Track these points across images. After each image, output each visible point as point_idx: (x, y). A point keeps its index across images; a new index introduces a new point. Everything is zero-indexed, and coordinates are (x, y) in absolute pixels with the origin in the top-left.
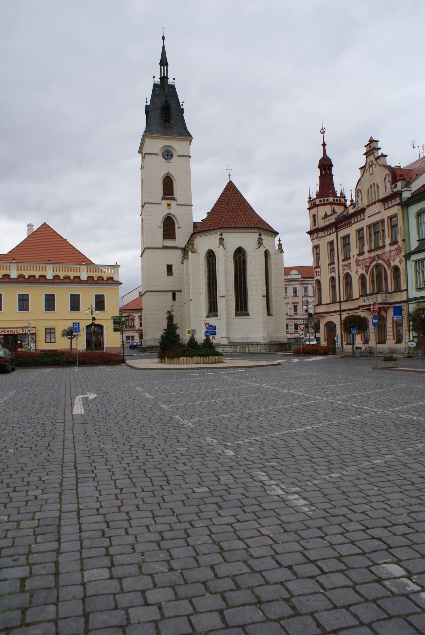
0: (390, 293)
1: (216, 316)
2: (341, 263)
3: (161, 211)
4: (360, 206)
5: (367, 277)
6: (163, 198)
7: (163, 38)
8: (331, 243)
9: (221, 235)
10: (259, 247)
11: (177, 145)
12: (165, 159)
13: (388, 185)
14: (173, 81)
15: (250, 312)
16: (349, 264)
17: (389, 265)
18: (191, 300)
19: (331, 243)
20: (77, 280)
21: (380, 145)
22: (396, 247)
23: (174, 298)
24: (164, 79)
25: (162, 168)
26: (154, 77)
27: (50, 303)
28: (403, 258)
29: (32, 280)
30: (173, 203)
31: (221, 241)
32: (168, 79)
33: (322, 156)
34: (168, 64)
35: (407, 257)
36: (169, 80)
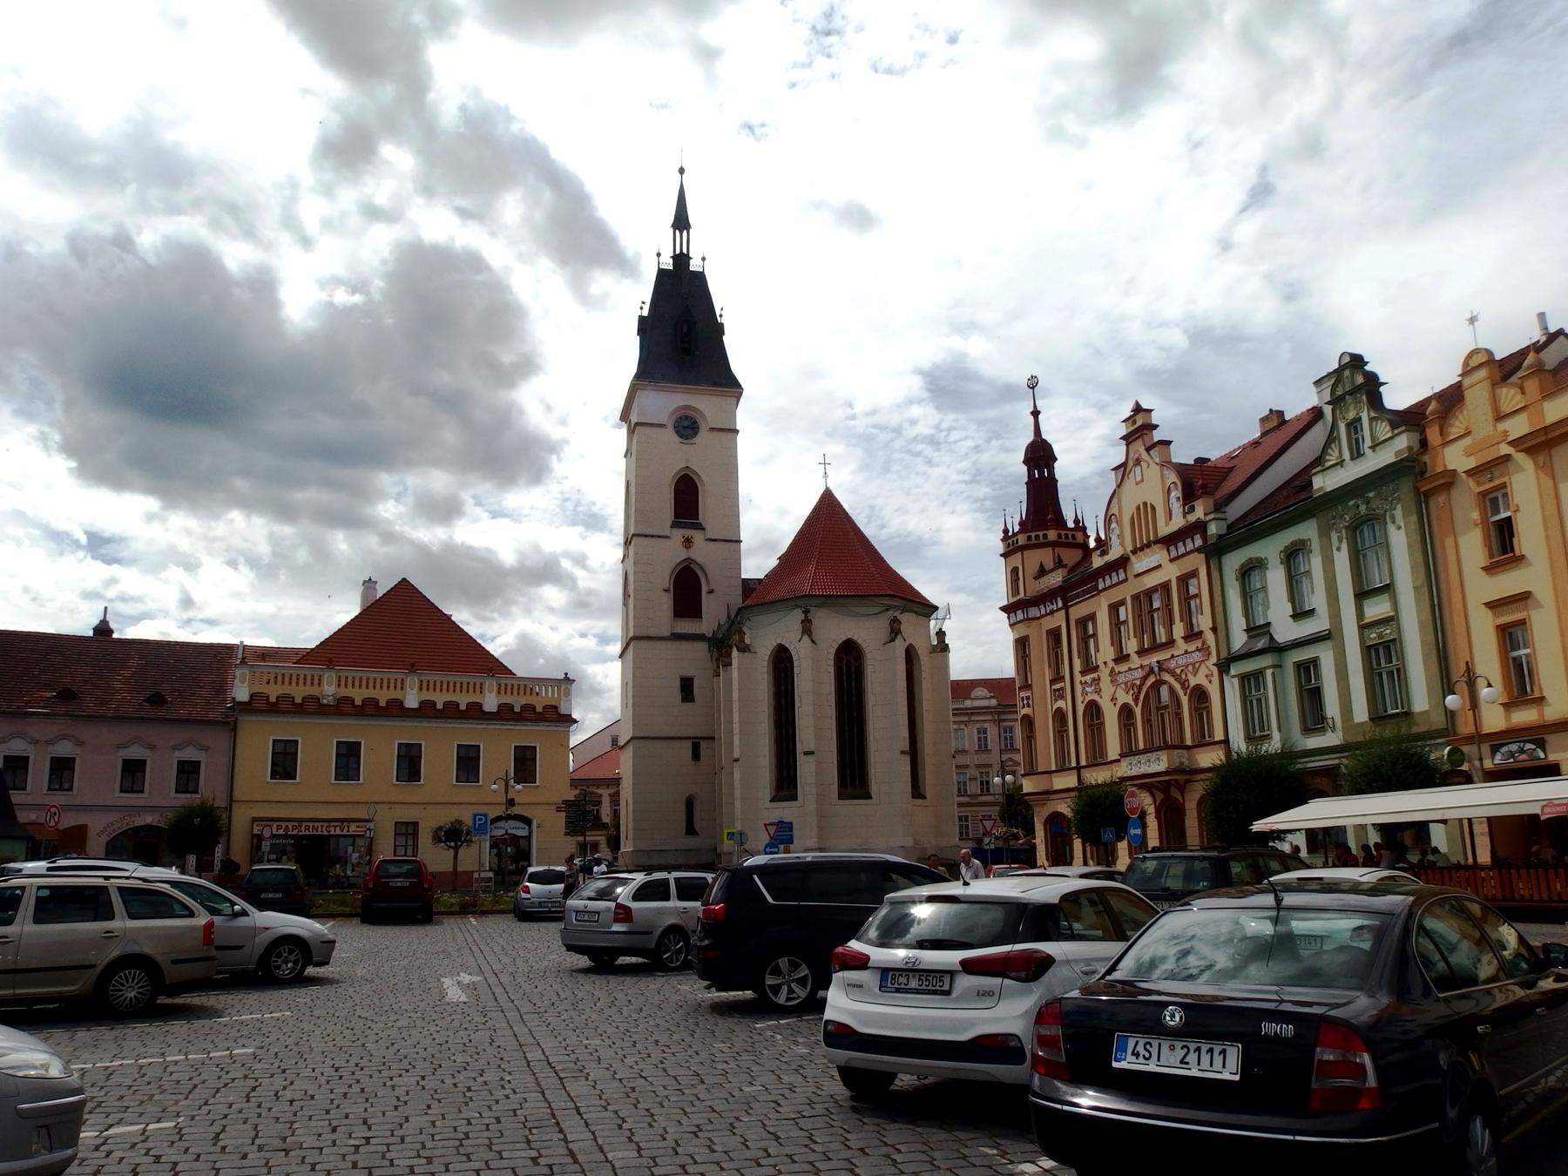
0: (1188, 748)
1: (794, 798)
2: (1078, 677)
3: (671, 553)
5: (1138, 711)
6: (675, 525)
7: (682, 171)
8: (1054, 635)
9: (806, 612)
10: (892, 640)
12: (681, 436)
13: (1177, 507)
15: (874, 790)
16: (1097, 681)
18: (736, 760)
19: (1054, 635)
20: (475, 712)
21: (1155, 418)
23: (696, 755)
24: (681, 259)
25: (675, 455)
26: (659, 255)
27: (410, 763)
28: (1215, 670)
29: (370, 709)
30: (697, 536)
33: (1030, 437)
35: (1223, 667)
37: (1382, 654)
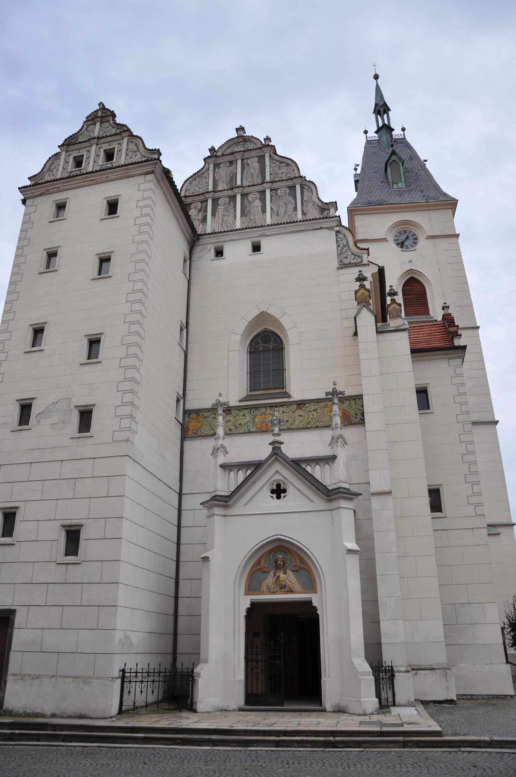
7: (376, 77)
11: (426, 221)
14: (402, 133)
26: (366, 132)
32: (393, 130)
34: (389, 110)
36: (394, 133)
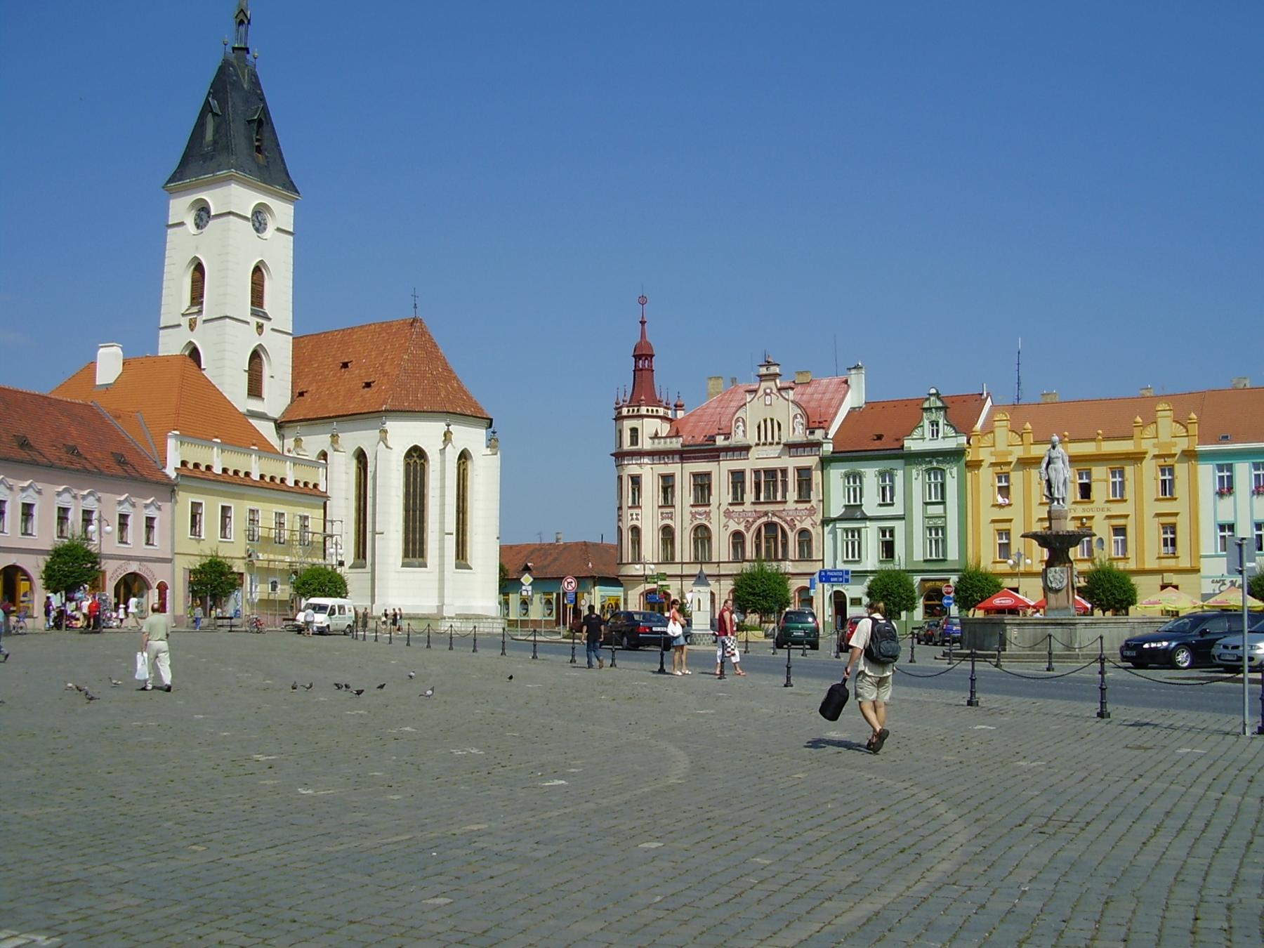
4: (737, 439)
5: (749, 537)
6: (254, 313)
13: (800, 429)
16: (708, 514)
17: (793, 528)
22: (808, 506)
31: (447, 436)
37: (937, 530)
